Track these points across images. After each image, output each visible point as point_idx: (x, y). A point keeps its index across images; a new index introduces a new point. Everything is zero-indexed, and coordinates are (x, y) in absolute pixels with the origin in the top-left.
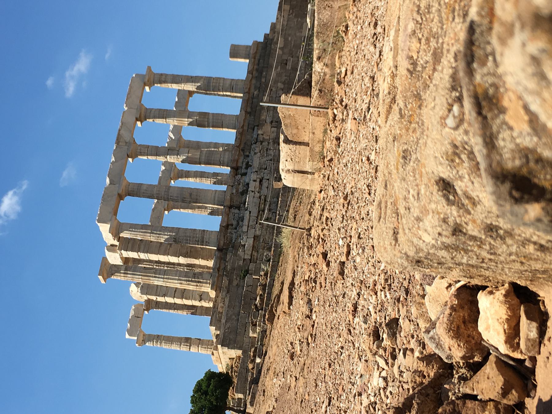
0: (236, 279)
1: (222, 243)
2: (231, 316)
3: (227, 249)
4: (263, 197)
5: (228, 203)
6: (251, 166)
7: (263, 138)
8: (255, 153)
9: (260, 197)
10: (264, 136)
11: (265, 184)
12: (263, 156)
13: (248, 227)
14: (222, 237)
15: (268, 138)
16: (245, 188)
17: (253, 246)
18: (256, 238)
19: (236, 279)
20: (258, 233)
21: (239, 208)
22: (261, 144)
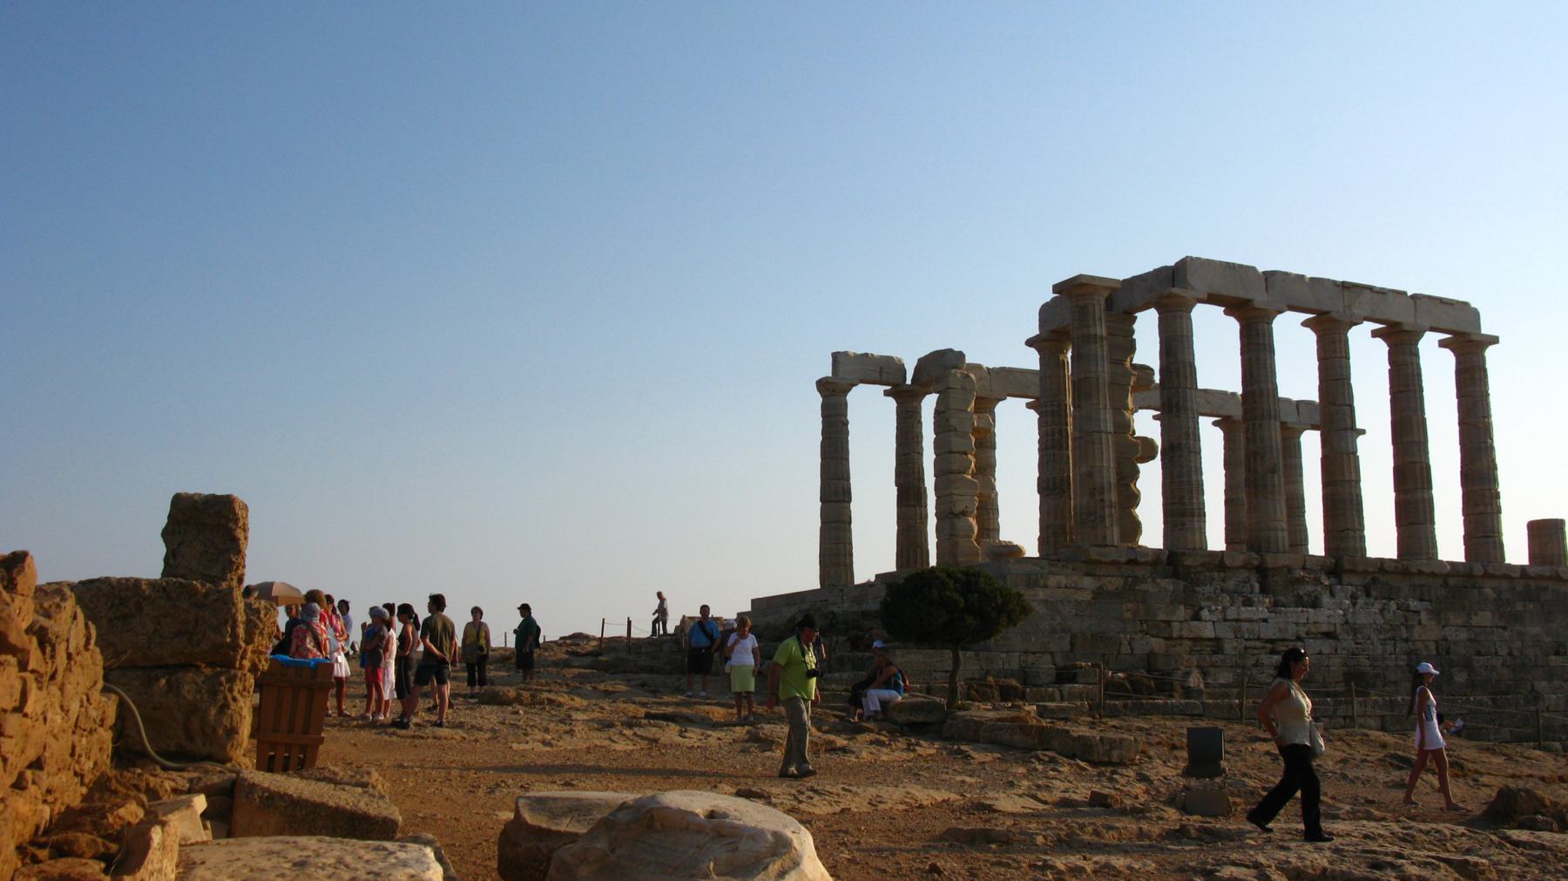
1: (1188, 562)
3: (1176, 575)
9: (1299, 639)
10: (1417, 628)
11: (1326, 646)
12: (1380, 631)
13: (1237, 620)
15: (1416, 636)
17: (1196, 640)
18: (1217, 645)
20: (1228, 647)
21: (1263, 591)
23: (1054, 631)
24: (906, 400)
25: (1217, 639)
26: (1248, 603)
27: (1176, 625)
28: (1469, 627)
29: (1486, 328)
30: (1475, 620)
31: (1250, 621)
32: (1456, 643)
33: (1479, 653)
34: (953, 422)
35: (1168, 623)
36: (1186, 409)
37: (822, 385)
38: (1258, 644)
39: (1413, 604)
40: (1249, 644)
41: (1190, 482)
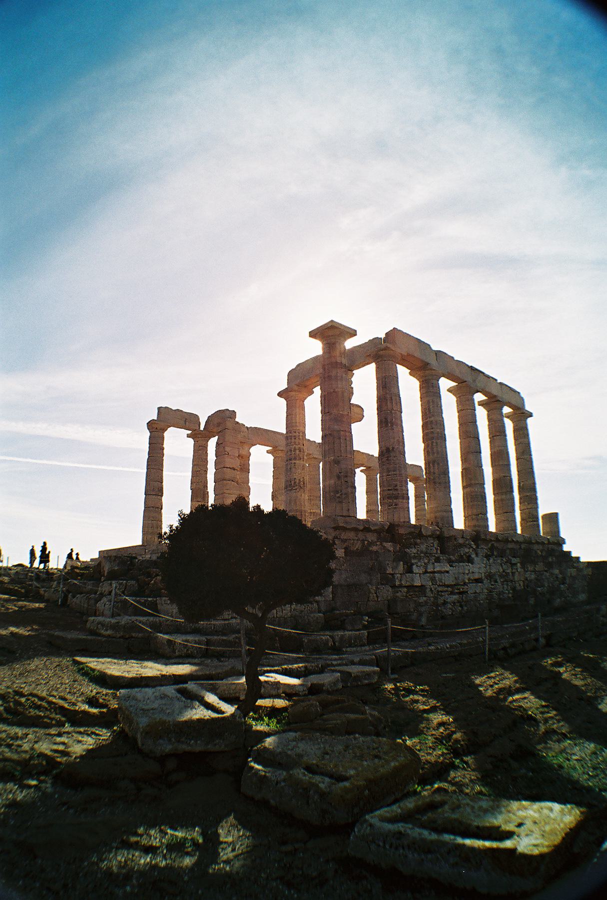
1: (402, 531)
3: (393, 540)
5: (446, 535)
9: (465, 584)
11: (478, 588)
12: (501, 576)
24: (200, 438)
25: (422, 586)
26: (438, 560)
28: (535, 571)
29: (528, 407)
31: (440, 572)
32: (531, 581)
34: (227, 449)
36: (397, 425)
37: (150, 425)
39: (514, 561)
41: (400, 475)
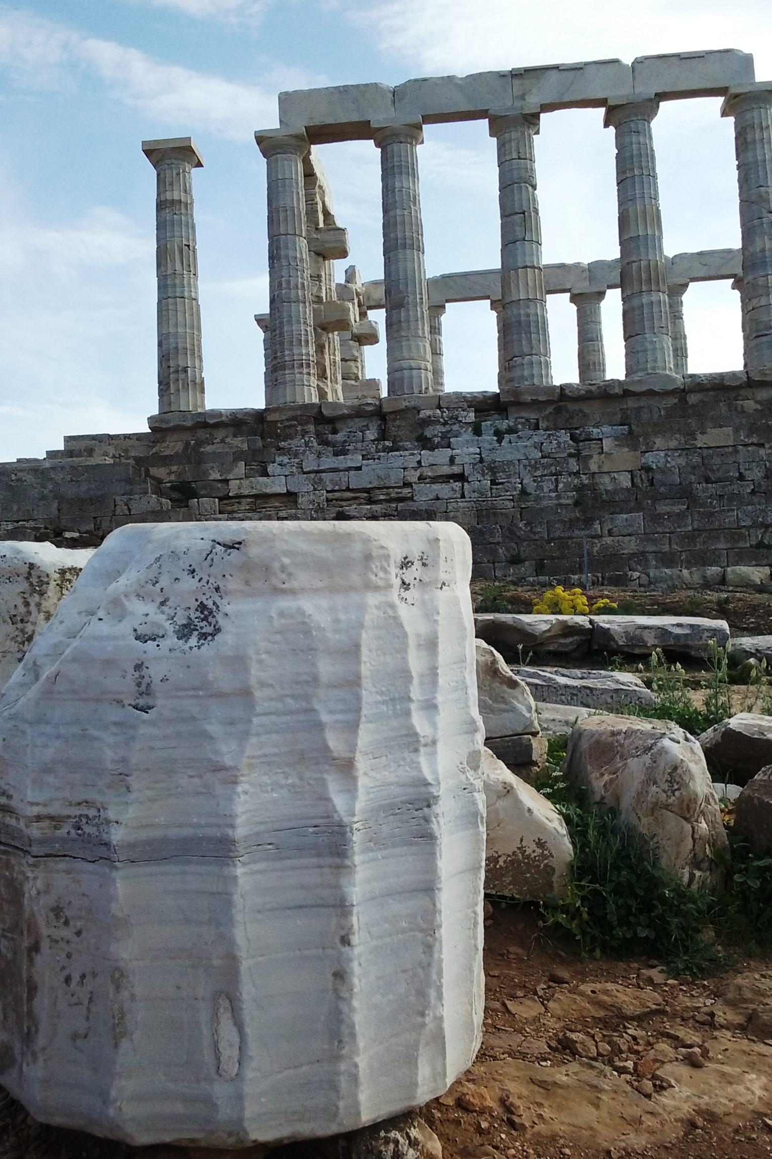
0: (170, 473)
2: (52, 479)
4: (406, 491)
6: (500, 441)
7: (591, 457)
8: (539, 446)
9: (407, 484)
12: (534, 466)
13: (317, 472)
14: (290, 414)
15: (594, 467)
16: (436, 440)
19: (170, 473)
21: (383, 435)
22: (570, 455)
23: (43, 498)
26: (341, 451)
27: (233, 484)
30: (701, 441)
32: (663, 471)
33: (708, 480)
35: (228, 480)
38: (349, 495)
40: (330, 495)
